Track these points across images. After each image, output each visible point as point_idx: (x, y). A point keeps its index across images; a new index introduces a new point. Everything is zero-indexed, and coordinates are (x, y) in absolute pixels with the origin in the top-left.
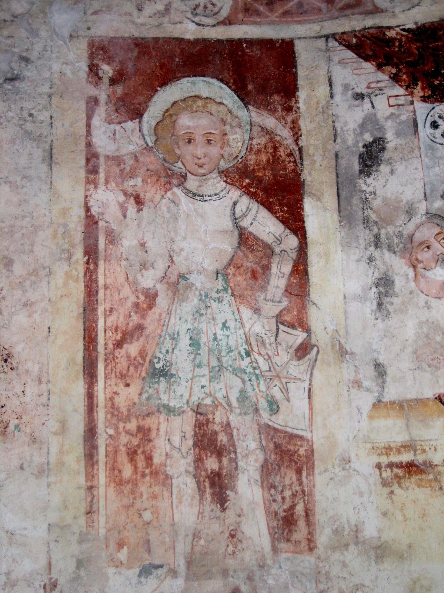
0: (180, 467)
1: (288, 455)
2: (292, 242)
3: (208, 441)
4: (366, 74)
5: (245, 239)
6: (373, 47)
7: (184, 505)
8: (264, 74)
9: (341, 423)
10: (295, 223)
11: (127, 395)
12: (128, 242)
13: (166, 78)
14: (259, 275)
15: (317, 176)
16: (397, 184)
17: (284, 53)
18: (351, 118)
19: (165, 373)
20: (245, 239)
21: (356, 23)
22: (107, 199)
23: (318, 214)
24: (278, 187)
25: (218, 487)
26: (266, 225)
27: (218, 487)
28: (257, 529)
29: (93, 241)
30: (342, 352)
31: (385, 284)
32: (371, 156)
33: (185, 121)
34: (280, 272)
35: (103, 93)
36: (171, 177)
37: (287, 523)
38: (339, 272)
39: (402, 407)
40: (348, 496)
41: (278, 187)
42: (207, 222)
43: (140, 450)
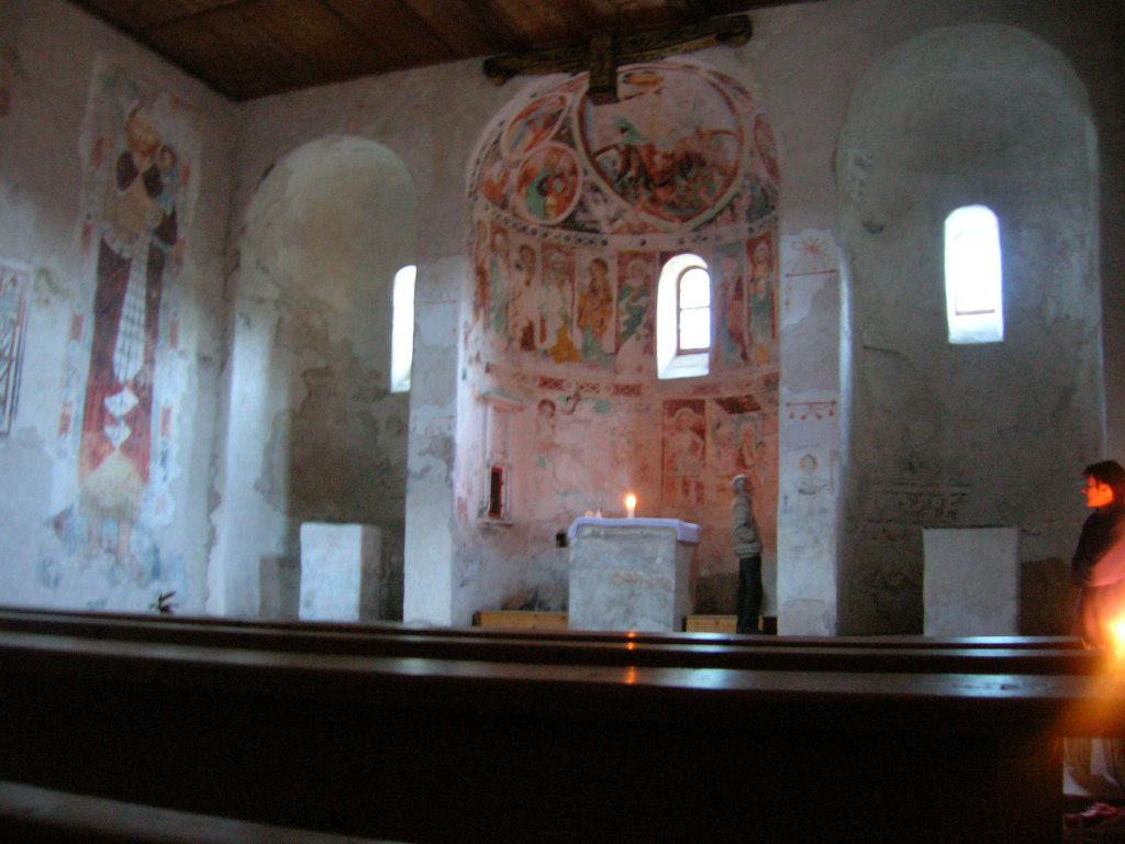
0: (680, 489)
1: (700, 486)
2: (702, 443)
3: (686, 484)
4: (719, 408)
5: (694, 442)
6: (720, 402)
7: (679, 494)
8: (698, 407)
9: (709, 480)
10: (703, 437)
11: (669, 475)
12: (671, 443)
13: (676, 409)
14: (696, 450)
15: (709, 428)
16: (724, 431)
17: (702, 403)
18: (715, 417)
19: (676, 470)
20: (694, 442)
21: (717, 396)
22: (666, 434)
23: (708, 437)
24: (701, 432)
25: (686, 492)
26: (698, 440)
27: (686, 492)
28: (694, 500)
29: (664, 443)
30: (711, 466)
31: (719, 453)
32: (719, 425)
33: (683, 417)
34: (701, 447)
35: (666, 412)
36: (679, 429)
37: (699, 499)
38: (711, 450)
39: (722, 477)
40: (710, 495)
41: (701, 432)
42: (686, 439)
43: (672, 484)
